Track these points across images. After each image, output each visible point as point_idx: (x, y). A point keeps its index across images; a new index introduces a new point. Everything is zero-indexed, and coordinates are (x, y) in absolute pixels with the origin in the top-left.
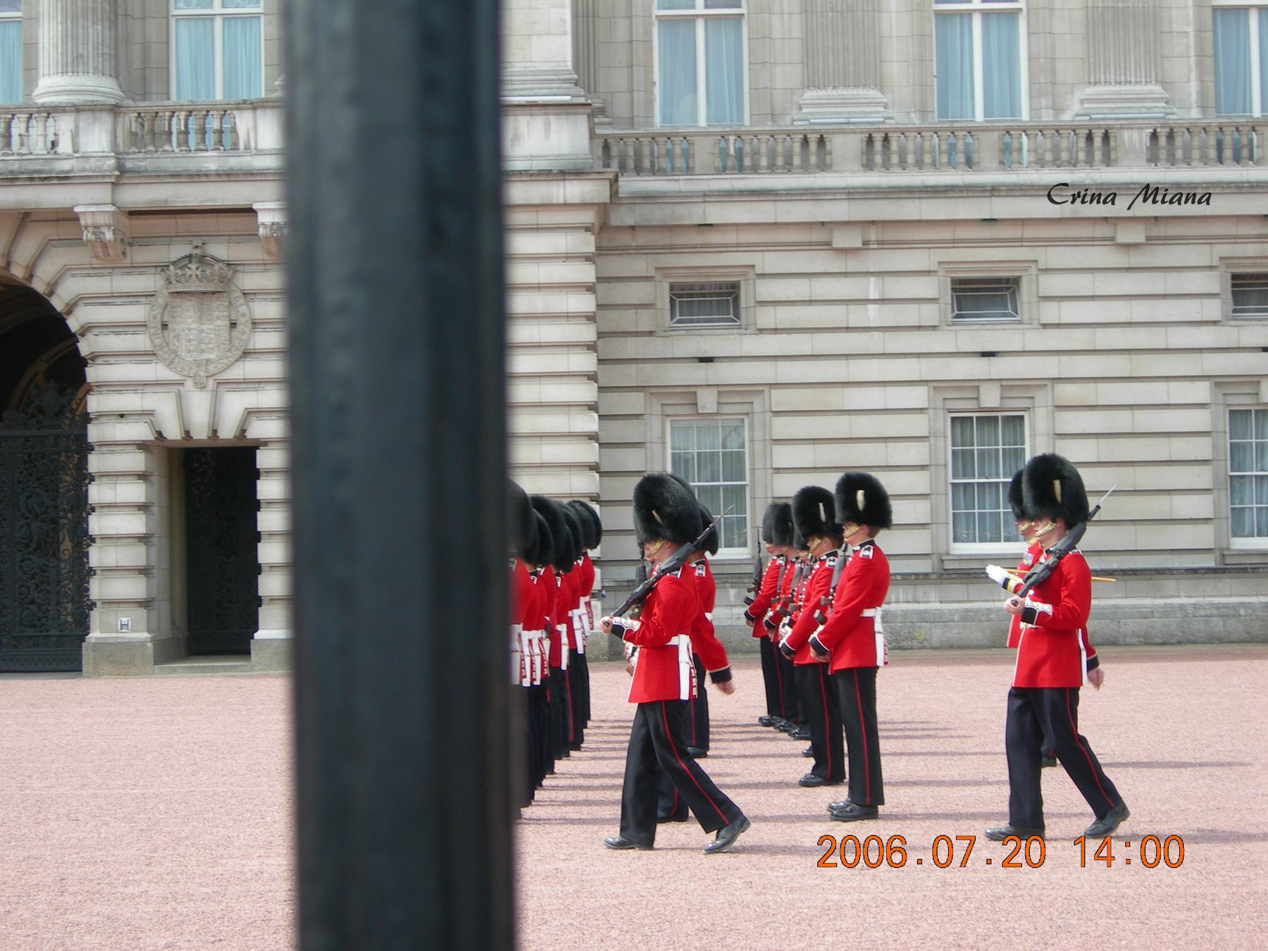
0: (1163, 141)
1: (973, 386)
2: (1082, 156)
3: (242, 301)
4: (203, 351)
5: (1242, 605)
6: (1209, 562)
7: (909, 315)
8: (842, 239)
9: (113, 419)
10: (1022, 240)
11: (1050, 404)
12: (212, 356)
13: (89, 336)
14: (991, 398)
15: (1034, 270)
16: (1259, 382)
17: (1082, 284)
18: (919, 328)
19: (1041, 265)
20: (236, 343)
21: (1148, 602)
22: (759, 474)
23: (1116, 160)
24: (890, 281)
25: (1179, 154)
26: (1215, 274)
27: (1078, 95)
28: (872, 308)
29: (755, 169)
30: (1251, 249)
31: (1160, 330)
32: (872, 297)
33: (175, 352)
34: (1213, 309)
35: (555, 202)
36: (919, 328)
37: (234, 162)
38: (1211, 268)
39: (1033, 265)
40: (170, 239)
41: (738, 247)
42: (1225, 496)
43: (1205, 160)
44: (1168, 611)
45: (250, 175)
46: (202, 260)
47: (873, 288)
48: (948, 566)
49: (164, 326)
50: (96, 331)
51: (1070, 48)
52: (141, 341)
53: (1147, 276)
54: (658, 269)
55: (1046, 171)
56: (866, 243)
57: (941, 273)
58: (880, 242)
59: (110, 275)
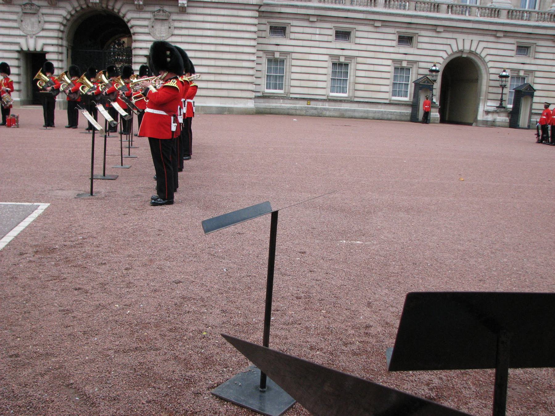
1: (338, 56)
3: (172, 22)
4: (162, 34)
5: (395, 112)
6: (387, 102)
7: (325, 38)
8: (312, 19)
9: (139, 49)
10: (353, 23)
11: (355, 62)
12: (164, 35)
13: (134, 28)
14: (342, 60)
15: (355, 30)
16: (402, 62)
18: (327, 42)
19: (357, 29)
20: (170, 32)
21: (375, 109)
22: (288, 73)
23: (377, 6)
24: (322, 30)
25: (391, 6)
28: (317, 36)
30: (404, 30)
31: (382, 47)
32: (317, 33)
33: (155, 34)
34: (394, 43)
35: (250, 3)
36: (327, 42)
38: (394, 34)
39: (355, 29)
41: (287, 18)
42: (391, 87)
43: (397, 8)
44: (379, 112)
46: (163, 11)
47: (318, 31)
48: (329, 98)
49: (153, 27)
50: (135, 27)
52: (146, 30)
53: (380, 34)
54: (268, 22)
55: (361, 7)
56: (317, 20)
57: (334, 29)
58: (320, 20)
59: (140, 13)
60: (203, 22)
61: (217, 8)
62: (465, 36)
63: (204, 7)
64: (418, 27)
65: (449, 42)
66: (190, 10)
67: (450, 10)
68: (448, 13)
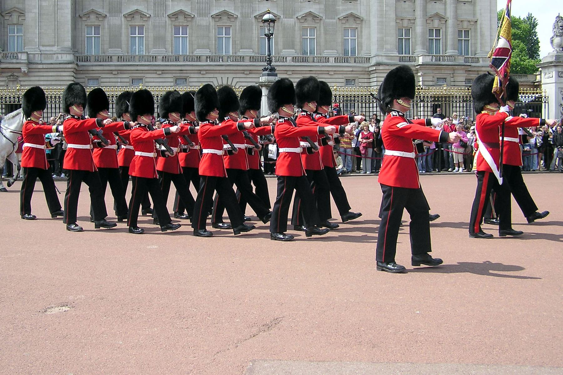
0: (164, 58)
2: (152, 60)
7: (125, 84)
17: (152, 80)
26: (173, 79)
27: (152, 50)
29: (100, 61)
30: (178, 75)
37: (18, 61)
40: (8, 72)
45: (21, 63)
49: (7, 86)
51: (151, 43)
56: (118, 73)
60: (39, 80)
61: (47, 72)
62: (223, 75)
63: (39, 72)
64: (188, 72)
65: (211, 80)
66: (30, 74)
67: (208, 59)
68: (207, 61)
